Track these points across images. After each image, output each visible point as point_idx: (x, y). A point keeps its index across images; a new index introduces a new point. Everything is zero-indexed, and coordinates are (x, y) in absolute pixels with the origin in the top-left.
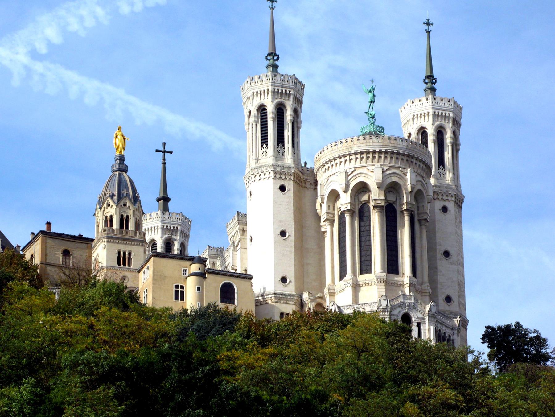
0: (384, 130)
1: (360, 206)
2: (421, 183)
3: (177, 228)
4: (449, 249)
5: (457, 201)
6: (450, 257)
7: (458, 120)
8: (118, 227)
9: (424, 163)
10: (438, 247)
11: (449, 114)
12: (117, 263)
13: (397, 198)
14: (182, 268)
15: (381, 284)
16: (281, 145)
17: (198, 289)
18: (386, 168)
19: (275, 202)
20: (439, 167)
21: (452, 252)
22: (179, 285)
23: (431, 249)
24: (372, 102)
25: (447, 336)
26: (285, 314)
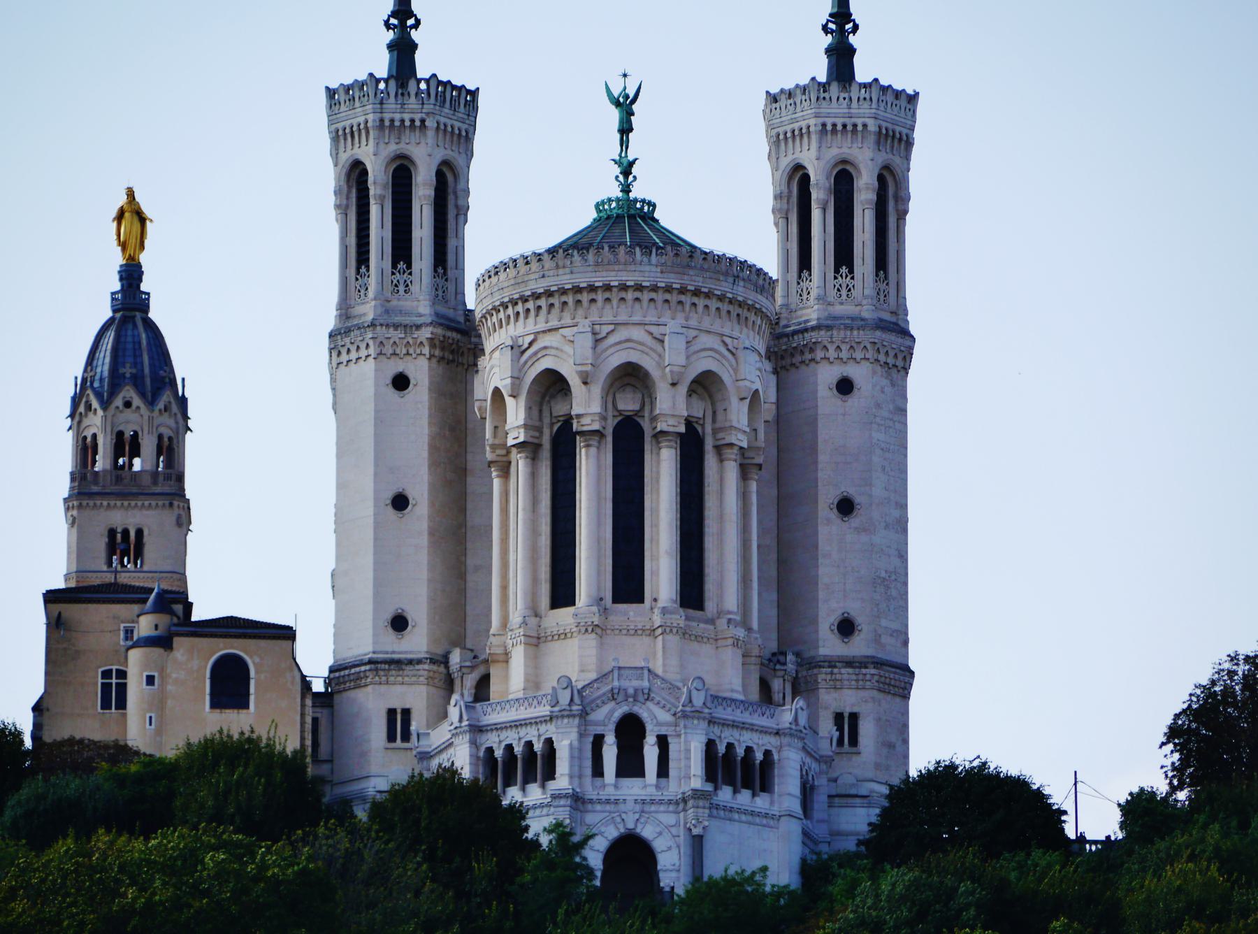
1: (555, 428)
2: (710, 353)
4: (852, 491)
5: (882, 358)
11: (865, 126)
13: (646, 400)
14: (122, 626)
15: (587, 636)
16: (401, 265)
17: (150, 680)
18: (606, 329)
19: (379, 421)
20: (837, 271)
22: (114, 668)
24: (625, 130)
25: (759, 756)
26: (399, 711)
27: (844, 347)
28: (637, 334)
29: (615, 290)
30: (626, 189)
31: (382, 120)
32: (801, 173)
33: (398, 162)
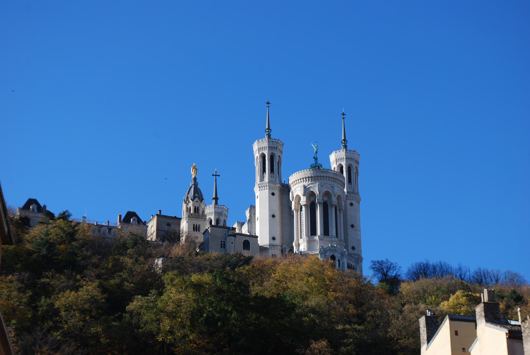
0: (322, 166)
3: (222, 212)
4: (353, 223)
6: (354, 227)
7: (358, 161)
8: (194, 212)
9: (342, 182)
10: (348, 223)
11: (354, 158)
12: (193, 229)
16: (272, 173)
17: (232, 243)
19: (269, 201)
20: (349, 184)
21: (355, 225)
22: (223, 240)
23: (345, 223)
27: (351, 197)
28: (329, 186)
29: (325, 177)
30: (316, 162)
31: (269, 146)
32: (341, 166)
33: (272, 154)
